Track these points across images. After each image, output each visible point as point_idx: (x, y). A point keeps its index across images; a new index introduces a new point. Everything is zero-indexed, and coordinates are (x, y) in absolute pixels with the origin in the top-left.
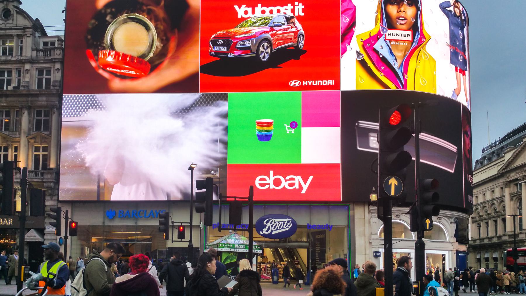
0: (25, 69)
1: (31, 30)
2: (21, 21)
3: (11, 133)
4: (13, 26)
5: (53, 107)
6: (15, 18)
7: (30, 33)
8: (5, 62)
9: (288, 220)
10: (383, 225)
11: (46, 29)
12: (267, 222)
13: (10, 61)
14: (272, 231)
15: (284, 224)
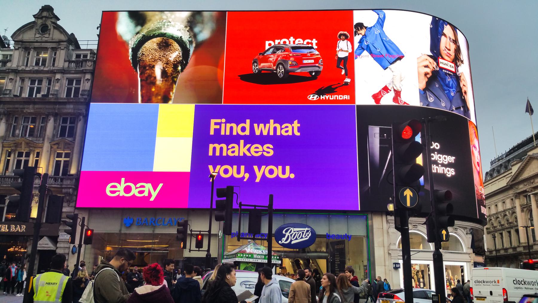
0: (56, 78)
1: (65, 43)
2: (57, 36)
3: (35, 139)
4: (49, 40)
5: (80, 114)
6: (51, 32)
7: (65, 46)
8: (37, 72)
9: (307, 229)
10: (401, 237)
11: (80, 43)
12: (286, 231)
13: (42, 71)
14: (291, 241)
15: (303, 233)
